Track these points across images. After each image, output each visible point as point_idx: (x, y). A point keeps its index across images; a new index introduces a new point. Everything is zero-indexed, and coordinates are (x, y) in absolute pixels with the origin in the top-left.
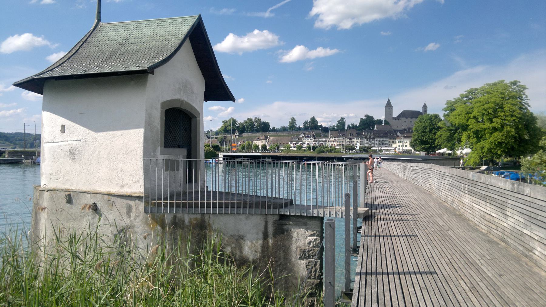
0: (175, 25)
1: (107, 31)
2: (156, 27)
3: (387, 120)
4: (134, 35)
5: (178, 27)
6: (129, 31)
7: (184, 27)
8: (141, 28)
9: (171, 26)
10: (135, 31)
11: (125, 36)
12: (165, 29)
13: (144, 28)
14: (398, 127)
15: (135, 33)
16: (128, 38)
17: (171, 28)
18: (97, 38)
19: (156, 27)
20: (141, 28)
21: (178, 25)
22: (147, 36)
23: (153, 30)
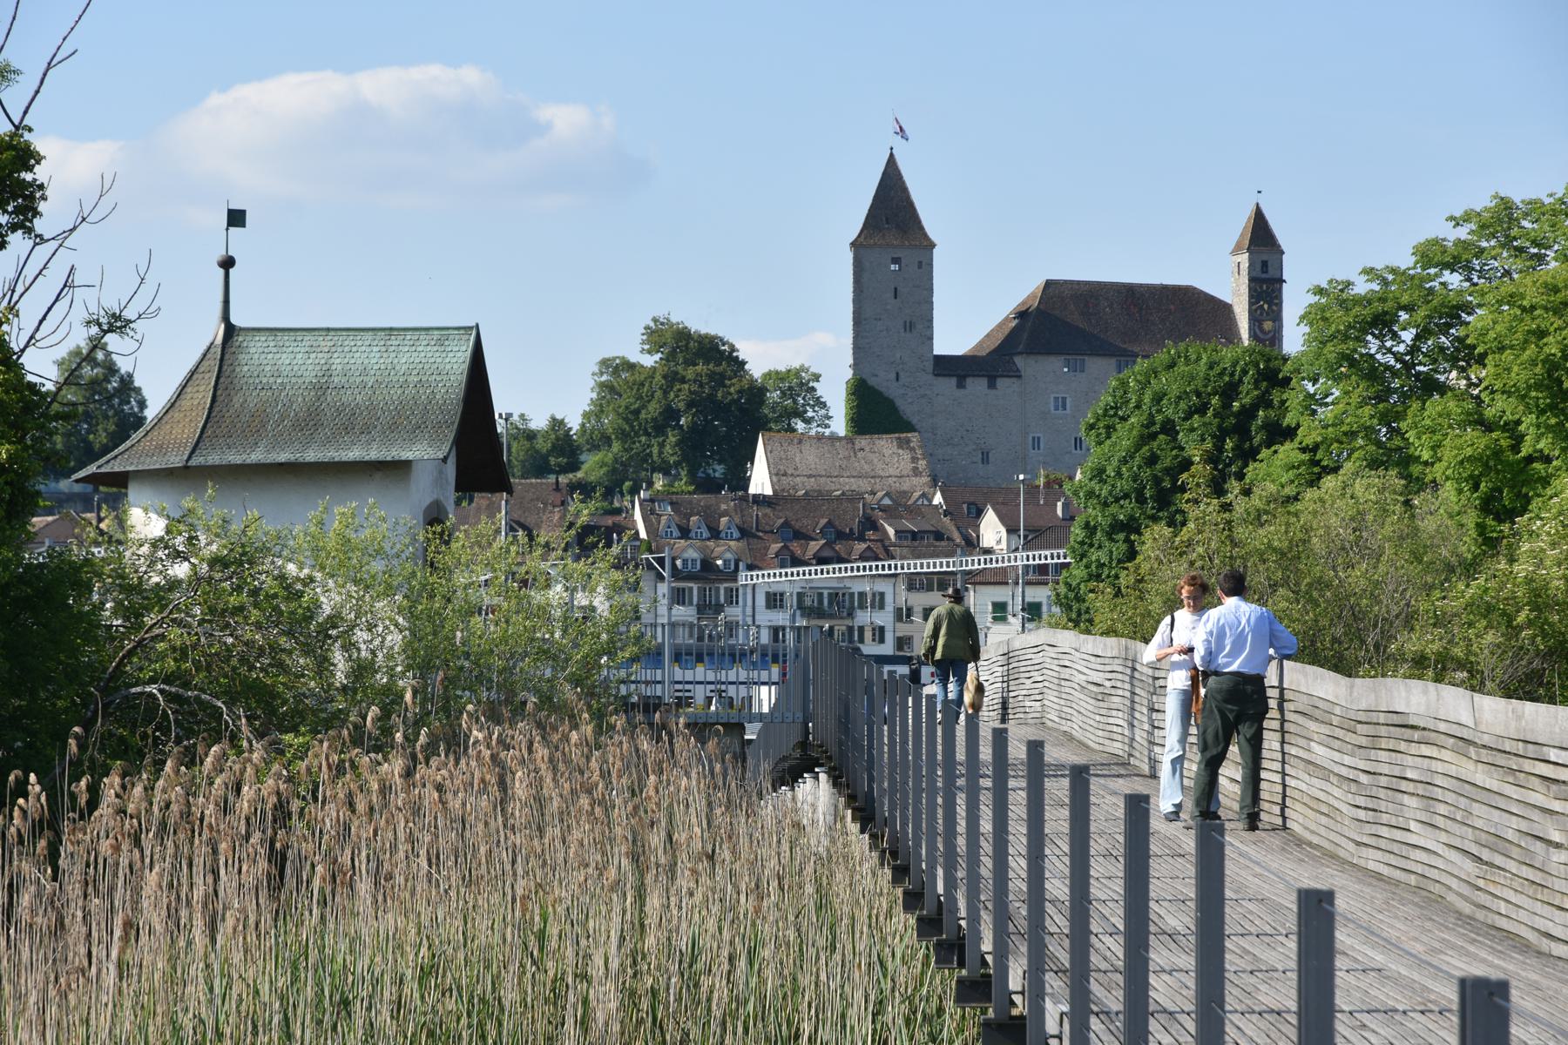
0: (429, 348)
1: (261, 350)
2: (384, 349)
3: (883, 381)
4: (339, 367)
5: (438, 354)
6: (320, 355)
7: (451, 355)
8: (346, 349)
9: (420, 349)
10: (336, 355)
11: (318, 368)
12: (408, 355)
13: (354, 349)
14: (985, 458)
15: (338, 361)
16: (328, 373)
17: (423, 354)
18: (246, 368)
19: (384, 349)
20: (346, 349)
21: (435, 348)
22: (373, 372)
23: (378, 355)
